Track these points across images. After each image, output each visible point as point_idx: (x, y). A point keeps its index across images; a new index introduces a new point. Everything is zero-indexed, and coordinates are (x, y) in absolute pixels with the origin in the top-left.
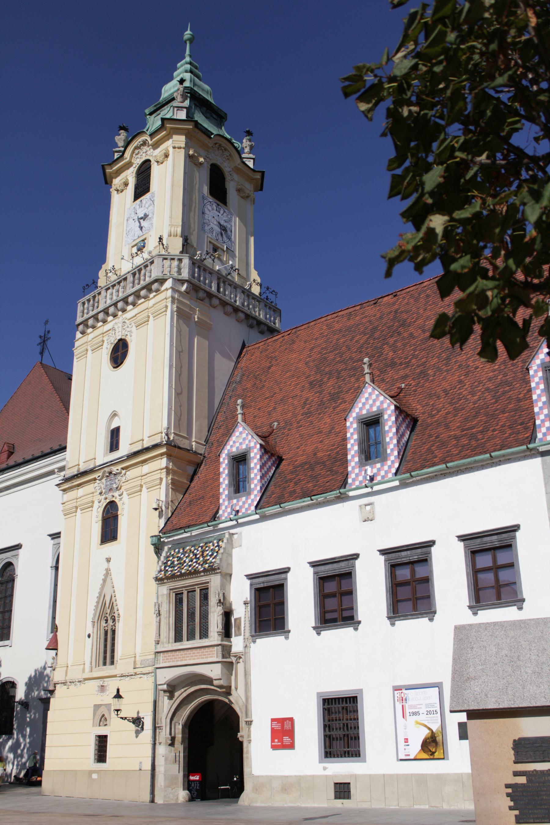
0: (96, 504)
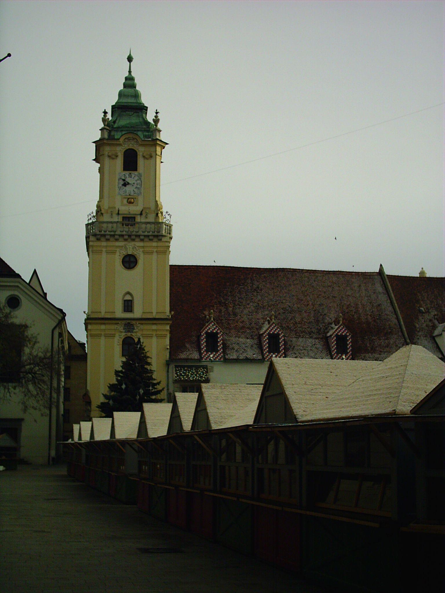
0: (117, 335)
